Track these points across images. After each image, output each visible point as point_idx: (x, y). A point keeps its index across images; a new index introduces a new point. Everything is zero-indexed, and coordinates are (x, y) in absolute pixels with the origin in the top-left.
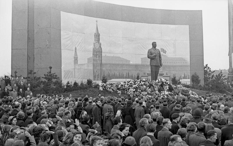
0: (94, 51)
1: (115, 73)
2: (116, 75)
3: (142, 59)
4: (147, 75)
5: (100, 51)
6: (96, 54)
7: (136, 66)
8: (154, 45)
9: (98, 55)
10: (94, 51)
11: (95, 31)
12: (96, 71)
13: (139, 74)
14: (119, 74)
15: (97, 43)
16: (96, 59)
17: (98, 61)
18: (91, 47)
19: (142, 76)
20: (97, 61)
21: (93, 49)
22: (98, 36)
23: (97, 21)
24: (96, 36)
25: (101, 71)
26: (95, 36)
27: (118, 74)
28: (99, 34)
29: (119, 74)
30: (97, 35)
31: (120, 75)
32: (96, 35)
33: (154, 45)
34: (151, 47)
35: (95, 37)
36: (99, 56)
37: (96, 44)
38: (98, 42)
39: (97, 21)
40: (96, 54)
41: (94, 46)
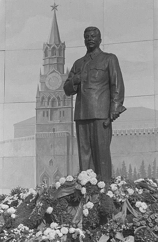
0: (43, 98)
1: (124, 164)
2: (133, 170)
6: (50, 107)
8: (92, 37)
9: (56, 109)
10: (40, 100)
11: (46, 37)
12: (51, 161)
14: (142, 167)
15: (54, 74)
16: (52, 122)
17: (57, 127)
18: (31, 91)
20: (54, 130)
21: (39, 92)
22: (57, 52)
24: (49, 54)
25: (68, 161)
26: (46, 52)
27: (136, 167)
28: (64, 44)
30: (54, 48)
33: (92, 37)
34: (83, 51)
35: (46, 55)
37: (50, 76)
38: (58, 69)
40: (50, 107)
41: (42, 83)
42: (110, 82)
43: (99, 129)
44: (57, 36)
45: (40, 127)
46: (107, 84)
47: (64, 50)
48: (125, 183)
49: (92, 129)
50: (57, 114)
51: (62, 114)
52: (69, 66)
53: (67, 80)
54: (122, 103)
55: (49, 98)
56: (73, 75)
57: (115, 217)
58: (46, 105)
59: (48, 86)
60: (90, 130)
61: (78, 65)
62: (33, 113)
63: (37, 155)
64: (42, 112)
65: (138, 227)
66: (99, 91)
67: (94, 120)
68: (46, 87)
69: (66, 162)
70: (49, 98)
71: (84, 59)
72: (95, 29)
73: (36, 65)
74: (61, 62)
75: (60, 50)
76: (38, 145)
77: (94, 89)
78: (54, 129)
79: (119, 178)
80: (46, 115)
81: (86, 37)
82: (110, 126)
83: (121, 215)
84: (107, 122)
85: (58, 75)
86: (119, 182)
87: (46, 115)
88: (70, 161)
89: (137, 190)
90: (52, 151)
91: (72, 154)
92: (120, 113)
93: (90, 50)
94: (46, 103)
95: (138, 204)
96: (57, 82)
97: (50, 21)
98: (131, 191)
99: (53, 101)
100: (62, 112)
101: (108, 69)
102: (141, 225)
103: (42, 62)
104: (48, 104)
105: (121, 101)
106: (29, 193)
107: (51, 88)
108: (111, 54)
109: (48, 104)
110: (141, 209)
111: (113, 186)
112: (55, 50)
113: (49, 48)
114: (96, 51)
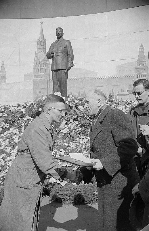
0: (37, 63)
3: (118, 67)
4: (126, 93)
5: (46, 63)
6: (39, 67)
7: (108, 80)
9: (42, 68)
10: (36, 64)
11: (37, 36)
12: (40, 91)
13: (113, 92)
14: (79, 94)
15: (41, 53)
18: (31, 60)
19: (117, 95)
21: (35, 61)
22: (43, 43)
23: (42, 23)
24: (39, 44)
25: (47, 91)
28: (46, 39)
29: (79, 94)
30: (41, 41)
31: (81, 95)
32: (39, 42)
34: (56, 38)
35: (38, 45)
36: (45, 71)
38: (43, 51)
39: (42, 23)
40: (39, 67)
41: (36, 57)
42: (67, 53)
43: (62, 74)
44: (43, 36)
45: (35, 76)
46: (66, 54)
47: (46, 42)
48: (74, 98)
49: (59, 74)
50: (42, 70)
51: (45, 70)
52: (47, 50)
53: (48, 52)
54: (73, 62)
55: (39, 64)
56: (51, 50)
57: (70, 113)
58: (38, 66)
59: (39, 58)
60: (58, 74)
61: (52, 46)
62: (32, 70)
63: (34, 88)
64: (36, 70)
65: (80, 117)
66: (62, 57)
67: (60, 70)
68: (38, 59)
69: (46, 91)
70: (39, 64)
71: (56, 42)
72: (61, 29)
73: (34, 49)
74: (45, 48)
75: (44, 42)
76: (34, 84)
77: (60, 56)
78: (41, 77)
79: (70, 96)
80: (38, 70)
81: (56, 32)
82: (66, 73)
83: (72, 112)
84: (66, 71)
85: (43, 53)
86: (71, 98)
87: (38, 70)
88: (48, 91)
89: (79, 101)
90: (40, 87)
91: (49, 88)
92: (72, 67)
93: (59, 38)
94: (38, 66)
95: (79, 107)
96: (44, 56)
97: (40, 29)
98: (76, 101)
99: (41, 65)
100: (45, 70)
101: (66, 47)
102: (81, 116)
103: (36, 48)
104: (39, 66)
105: (72, 61)
106: (31, 103)
107: (40, 59)
108: (68, 40)
109: (39, 66)
110: (81, 110)
111: (69, 99)
112: (42, 42)
113: (39, 41)
114: (61, 39)
